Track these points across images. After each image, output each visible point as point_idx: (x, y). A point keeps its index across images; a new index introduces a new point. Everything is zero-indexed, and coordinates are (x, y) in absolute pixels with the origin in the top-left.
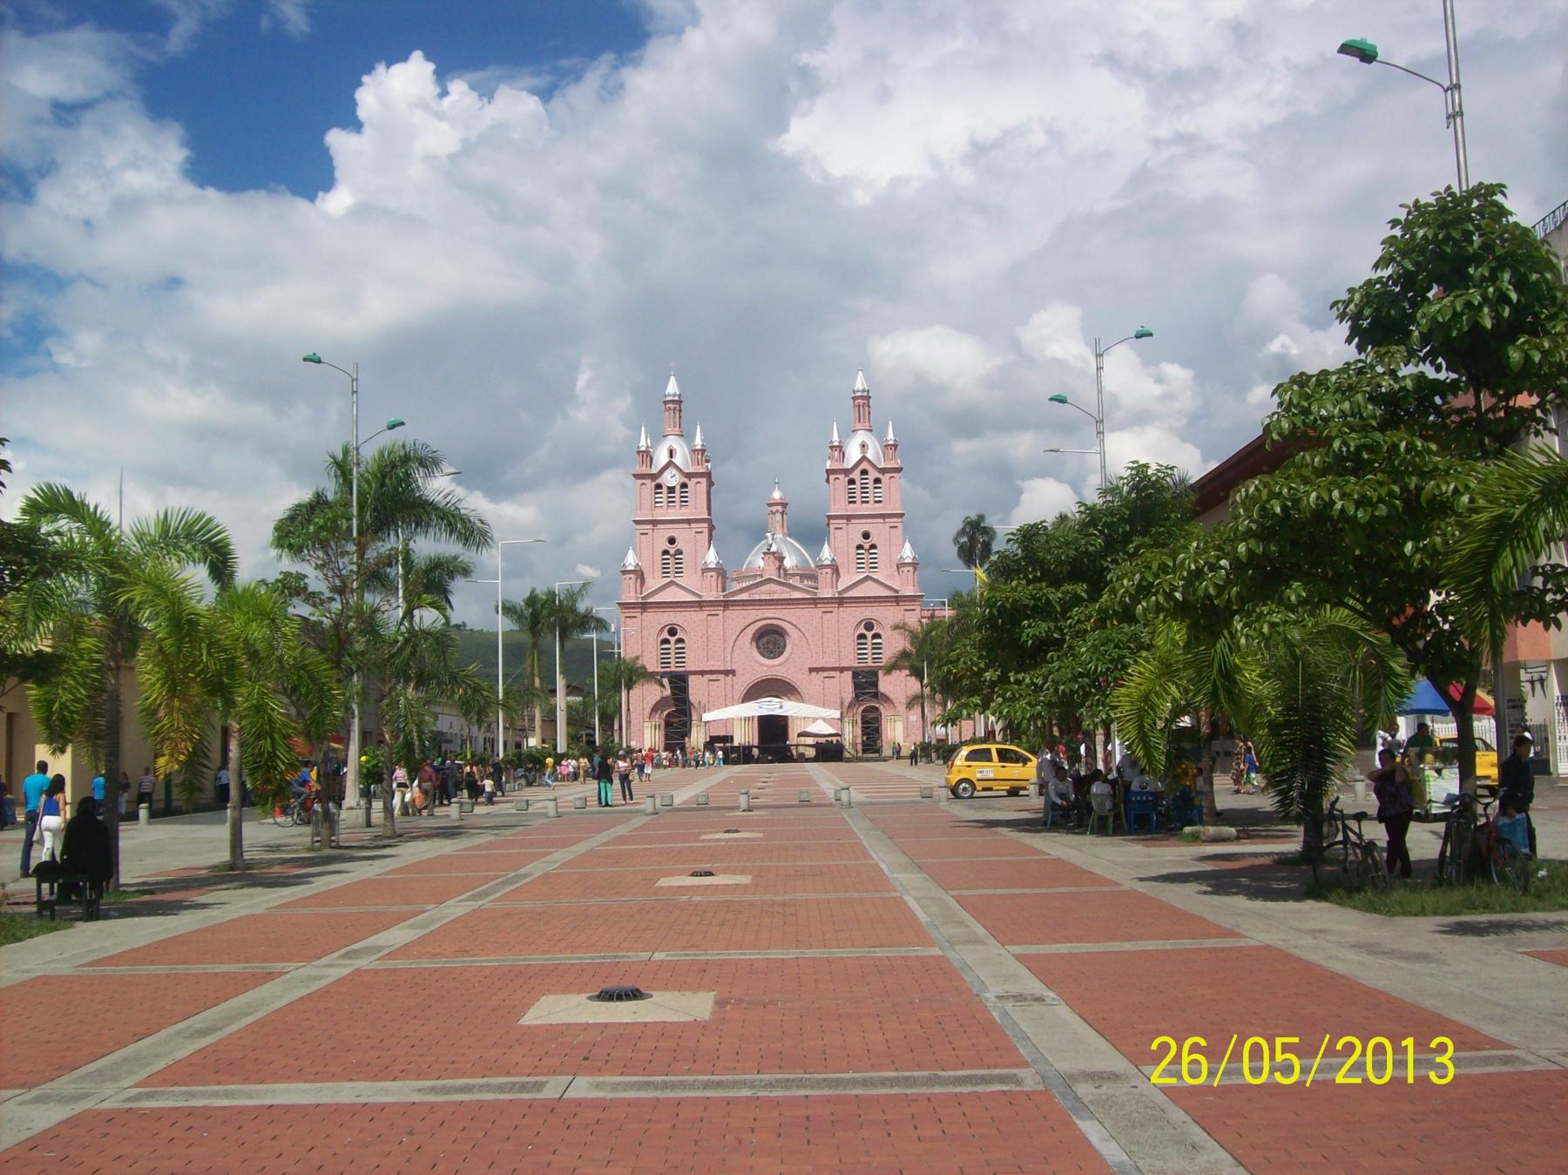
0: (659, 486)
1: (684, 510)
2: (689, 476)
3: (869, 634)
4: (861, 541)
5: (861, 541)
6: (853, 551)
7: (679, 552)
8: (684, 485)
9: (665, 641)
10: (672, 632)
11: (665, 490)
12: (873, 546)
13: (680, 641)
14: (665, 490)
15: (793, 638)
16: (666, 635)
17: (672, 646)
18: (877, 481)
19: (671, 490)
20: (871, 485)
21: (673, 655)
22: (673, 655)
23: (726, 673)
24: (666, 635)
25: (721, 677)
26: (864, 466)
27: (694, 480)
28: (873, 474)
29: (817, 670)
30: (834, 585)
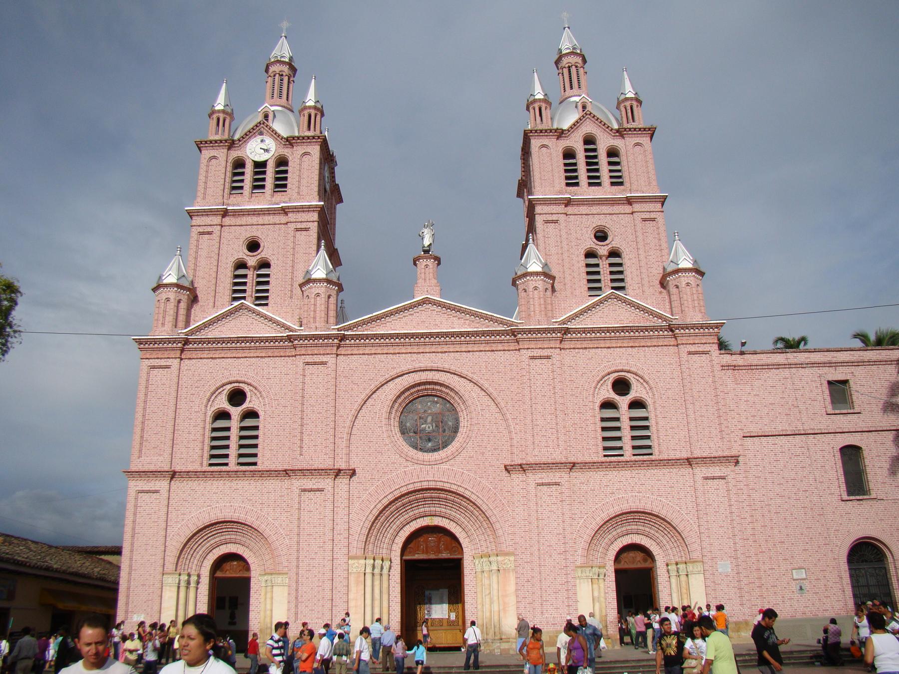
0: (239, 164)
1: (278, 197)
2: (290, 142)
3: (623, 402)
4: (590, 243)
5: (590, 243)
6: (582, 261)
7: (265, 264)
8: (282, 162)
9: (223, 415)
10: (237, 396)
11: (249, 170)
12: (614, 253)
13: (252, 414)
14: (249, 170)
15: (476, 416)
16: (222, 403)
17: (234, 424)
18: (612, 153)
19: (260, 166)
20: (603, 159)
21: (234, 442)
22: (234, 442)
23: (338, 473)
24: (222, 403)
25: (326, 483)
26: (589, 128)
27: (299, 150)
28: (604, 143)
29: (522, 468)
30: (548, 310)
